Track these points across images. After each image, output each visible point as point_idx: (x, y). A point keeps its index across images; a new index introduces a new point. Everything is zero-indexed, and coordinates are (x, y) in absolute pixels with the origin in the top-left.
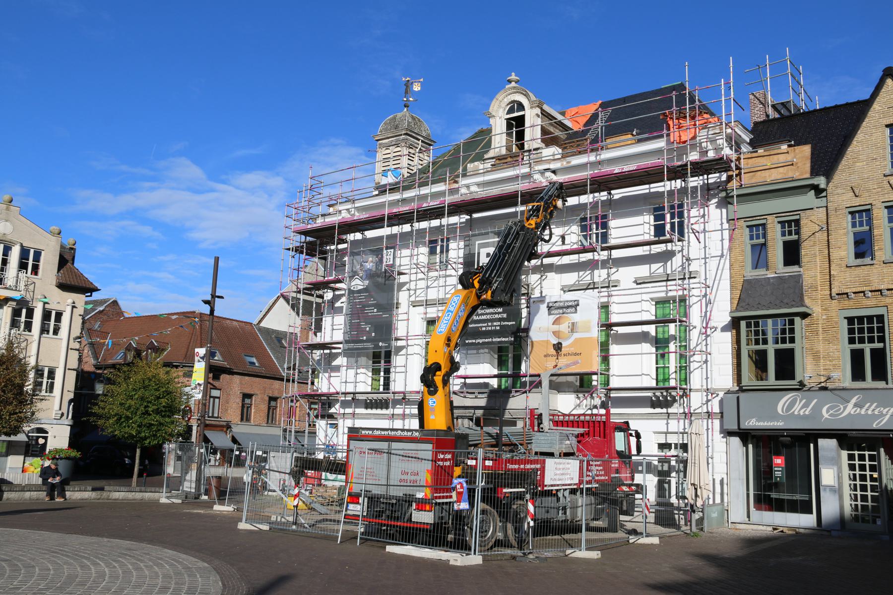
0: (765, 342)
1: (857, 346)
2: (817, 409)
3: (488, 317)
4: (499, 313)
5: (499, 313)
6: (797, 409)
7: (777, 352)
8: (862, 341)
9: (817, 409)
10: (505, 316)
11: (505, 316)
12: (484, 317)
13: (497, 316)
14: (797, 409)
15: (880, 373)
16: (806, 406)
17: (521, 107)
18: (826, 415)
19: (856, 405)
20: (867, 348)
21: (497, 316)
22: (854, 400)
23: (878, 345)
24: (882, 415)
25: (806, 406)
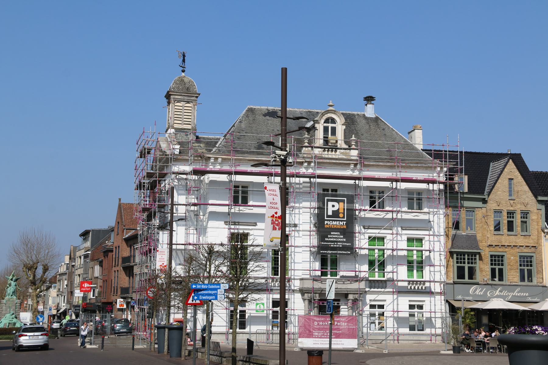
0: (464, 263)
1: (493, 267)
2: (485, 293)
3: (335, 239)
4: (341, 238)
5: (341, 238)
6: (477, 292)
7: (469, 268)
8: (495, 265)
9: (485, 293)
10: (345, 240)
11: (345, 240)
12: (332, 239)
13: (340, 240)
14: (477, 292)
15: (501, 279)
16: (481, 291)
17: (333, 121)
18: (489, 295)
19: (500, 291)
20: (497, 267)
21: (340, 240)
22: (499, 289)
23: (500, 267)
24: (509, 296)
25: (481, 291)
